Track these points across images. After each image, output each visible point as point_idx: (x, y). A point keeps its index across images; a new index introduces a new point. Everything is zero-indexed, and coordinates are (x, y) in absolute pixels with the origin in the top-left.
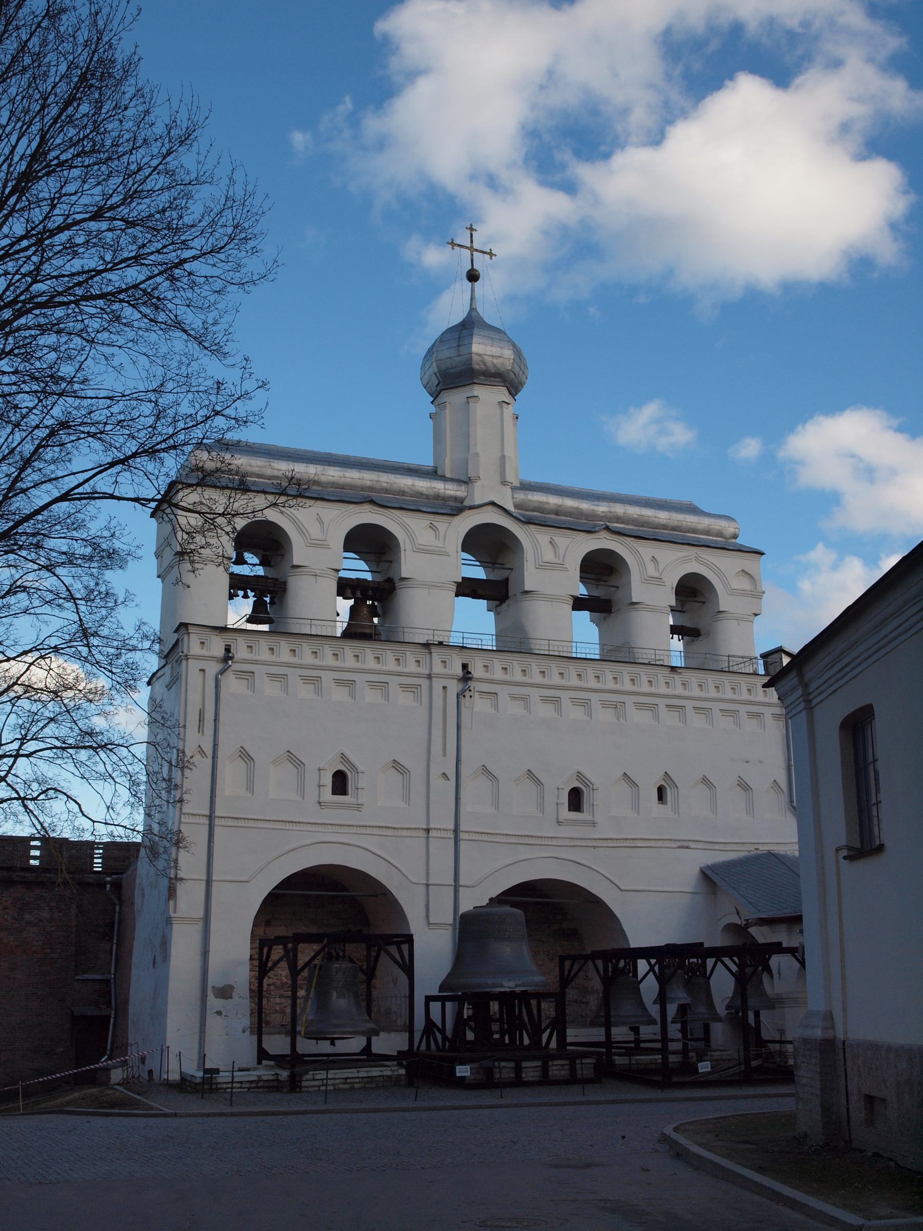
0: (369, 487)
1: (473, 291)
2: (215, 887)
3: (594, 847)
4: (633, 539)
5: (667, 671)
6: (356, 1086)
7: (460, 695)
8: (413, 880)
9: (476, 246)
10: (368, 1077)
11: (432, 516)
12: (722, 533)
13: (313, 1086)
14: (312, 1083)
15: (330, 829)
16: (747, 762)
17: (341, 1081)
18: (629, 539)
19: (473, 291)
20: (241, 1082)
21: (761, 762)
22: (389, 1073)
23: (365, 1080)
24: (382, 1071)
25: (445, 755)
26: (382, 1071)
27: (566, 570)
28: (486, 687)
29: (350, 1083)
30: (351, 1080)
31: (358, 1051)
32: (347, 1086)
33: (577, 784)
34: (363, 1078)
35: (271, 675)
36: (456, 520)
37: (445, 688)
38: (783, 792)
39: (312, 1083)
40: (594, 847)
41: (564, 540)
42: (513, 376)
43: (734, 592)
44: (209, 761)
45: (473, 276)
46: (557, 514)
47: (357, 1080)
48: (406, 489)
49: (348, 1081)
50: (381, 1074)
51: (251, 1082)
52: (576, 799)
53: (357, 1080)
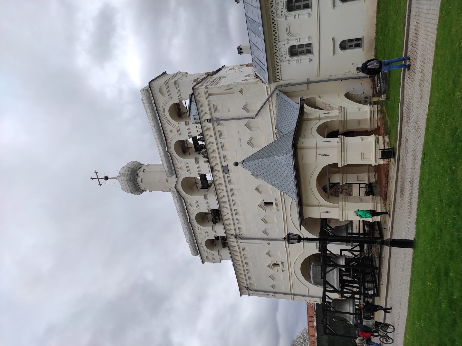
0: (185, 217)
1: (111, 178)
2: (311, 294)
3: (285, 199)
4: (167, 140)
5: (214, 172)
7: (242, 238)
8: (303, 252)
9: (97, 179)
11: (187, 205)
12: (148, 97)
15: (290, 270)
16: (240, 139)
18: (168, 142)
19: (110, 178)
21: (239, 133)
25: (262, 243)
27: (187, 164)
28: (237, 231)
33: (263, 204)
35: (249, 279)
36: (186, 198)
37: (241, 242)
38: (249, 120)
40: (285, 199)
41: (178, 165)
42: (131, 178)
43: (170, 96)
44: (276, 294)
45: (106, 178)
46: (170, 161)
48: (182, 208)
52: (268, 204)
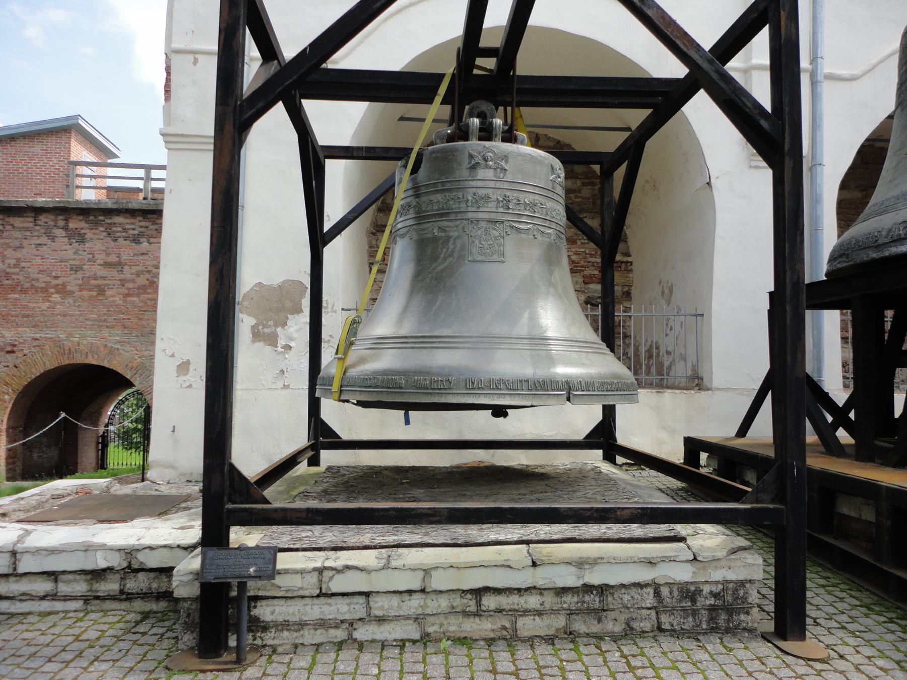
6: (528, 626)
10: (588, 588)
13: (322, 624)
14: (315, 610)
17: (458, 602)
20: (53, 575)
22: (683, 574)
23: (570, 600)
24: (651, 563)
26: (651, 563)
29: (499, 611)
30: (504, 601)
31: (580, 436)
32: (485, 627)
34: (563, 591)
39: (315, 610)
47: (533, 601)
49: (489, 602)
50: (645, 575)
51: (97, 574)
53: (533, 601)
